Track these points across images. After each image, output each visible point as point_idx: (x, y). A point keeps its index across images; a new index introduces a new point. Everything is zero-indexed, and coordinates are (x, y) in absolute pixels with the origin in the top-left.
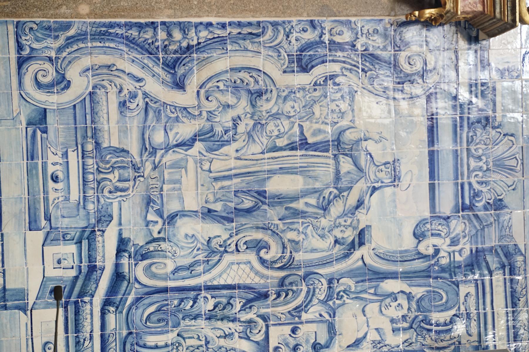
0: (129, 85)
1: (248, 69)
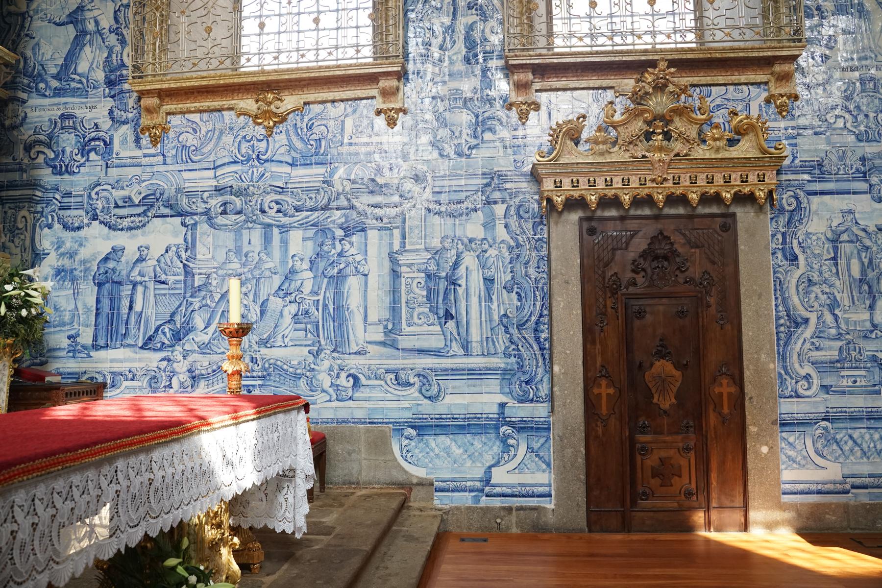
0: (808, 345)
1: (797, 286)
